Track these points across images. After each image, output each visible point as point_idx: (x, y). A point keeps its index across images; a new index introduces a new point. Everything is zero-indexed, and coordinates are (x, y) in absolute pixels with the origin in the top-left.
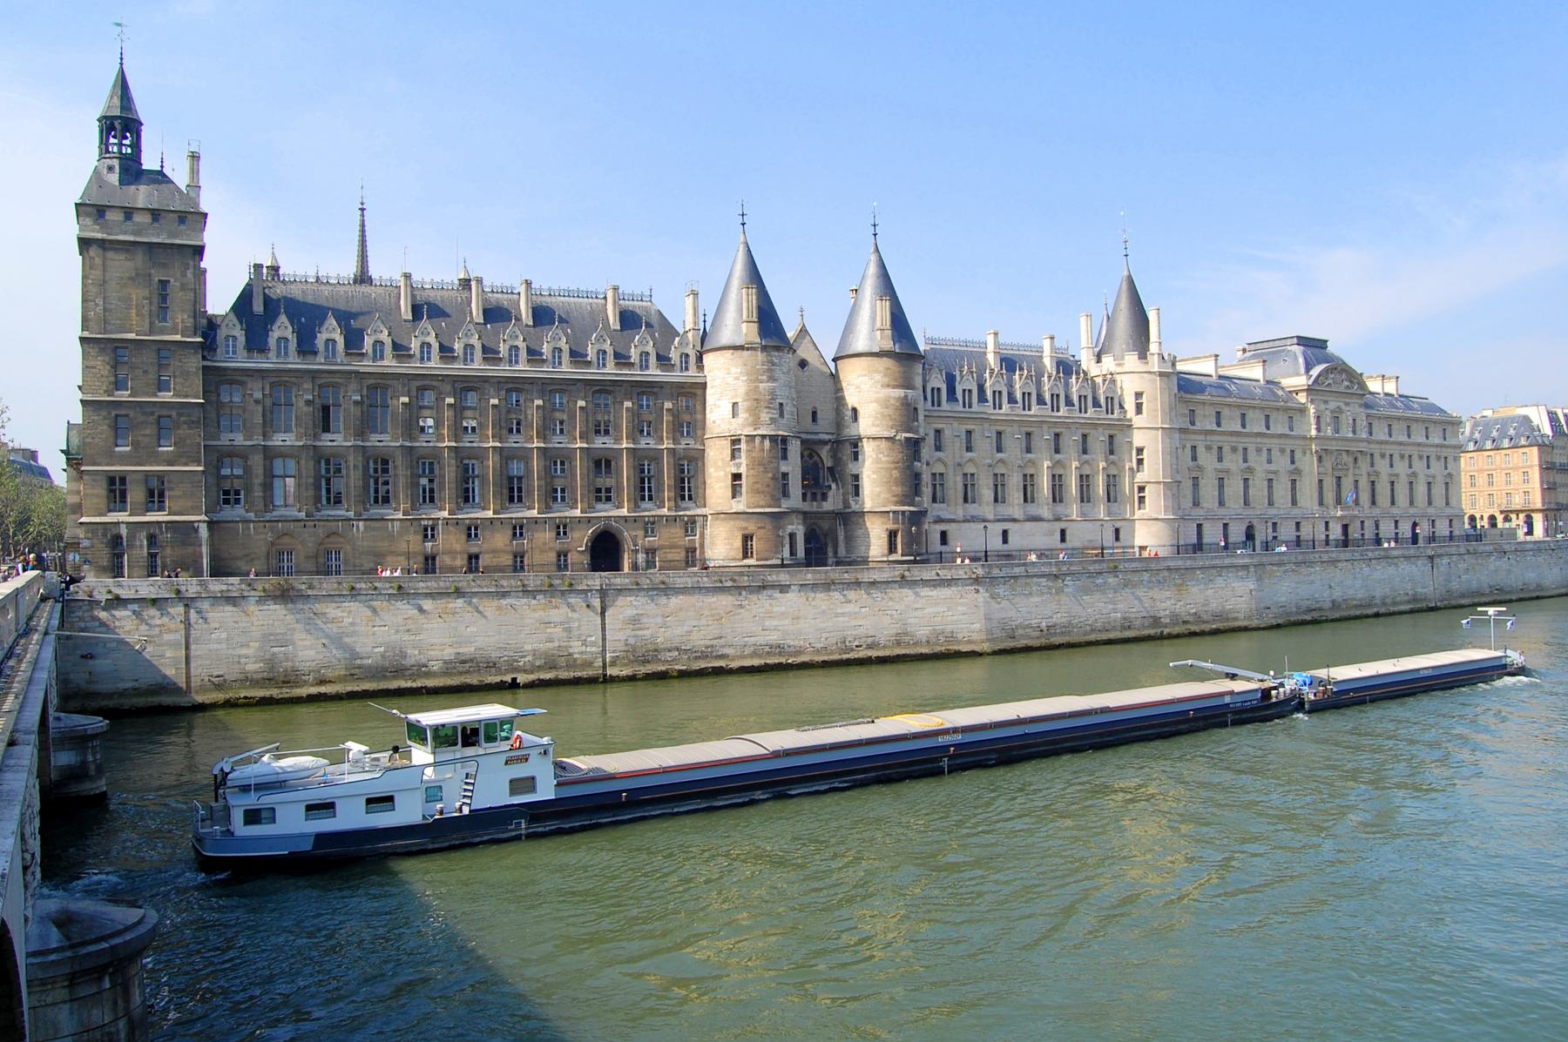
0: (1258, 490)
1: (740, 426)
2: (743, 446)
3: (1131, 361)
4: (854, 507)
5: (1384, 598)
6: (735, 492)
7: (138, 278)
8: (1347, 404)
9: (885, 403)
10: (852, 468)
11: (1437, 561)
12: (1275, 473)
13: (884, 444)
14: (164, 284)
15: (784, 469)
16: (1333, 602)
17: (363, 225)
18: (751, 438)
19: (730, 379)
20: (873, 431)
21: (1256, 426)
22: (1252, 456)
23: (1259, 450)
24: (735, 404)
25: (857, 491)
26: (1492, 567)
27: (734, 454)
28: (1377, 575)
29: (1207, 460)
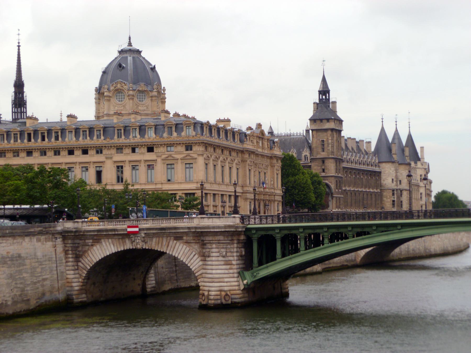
1: (393, 186)
2: (395, 192)
7: (337, 140)
18: (397, 190)
24: (393, 179)
27: (393, 194)
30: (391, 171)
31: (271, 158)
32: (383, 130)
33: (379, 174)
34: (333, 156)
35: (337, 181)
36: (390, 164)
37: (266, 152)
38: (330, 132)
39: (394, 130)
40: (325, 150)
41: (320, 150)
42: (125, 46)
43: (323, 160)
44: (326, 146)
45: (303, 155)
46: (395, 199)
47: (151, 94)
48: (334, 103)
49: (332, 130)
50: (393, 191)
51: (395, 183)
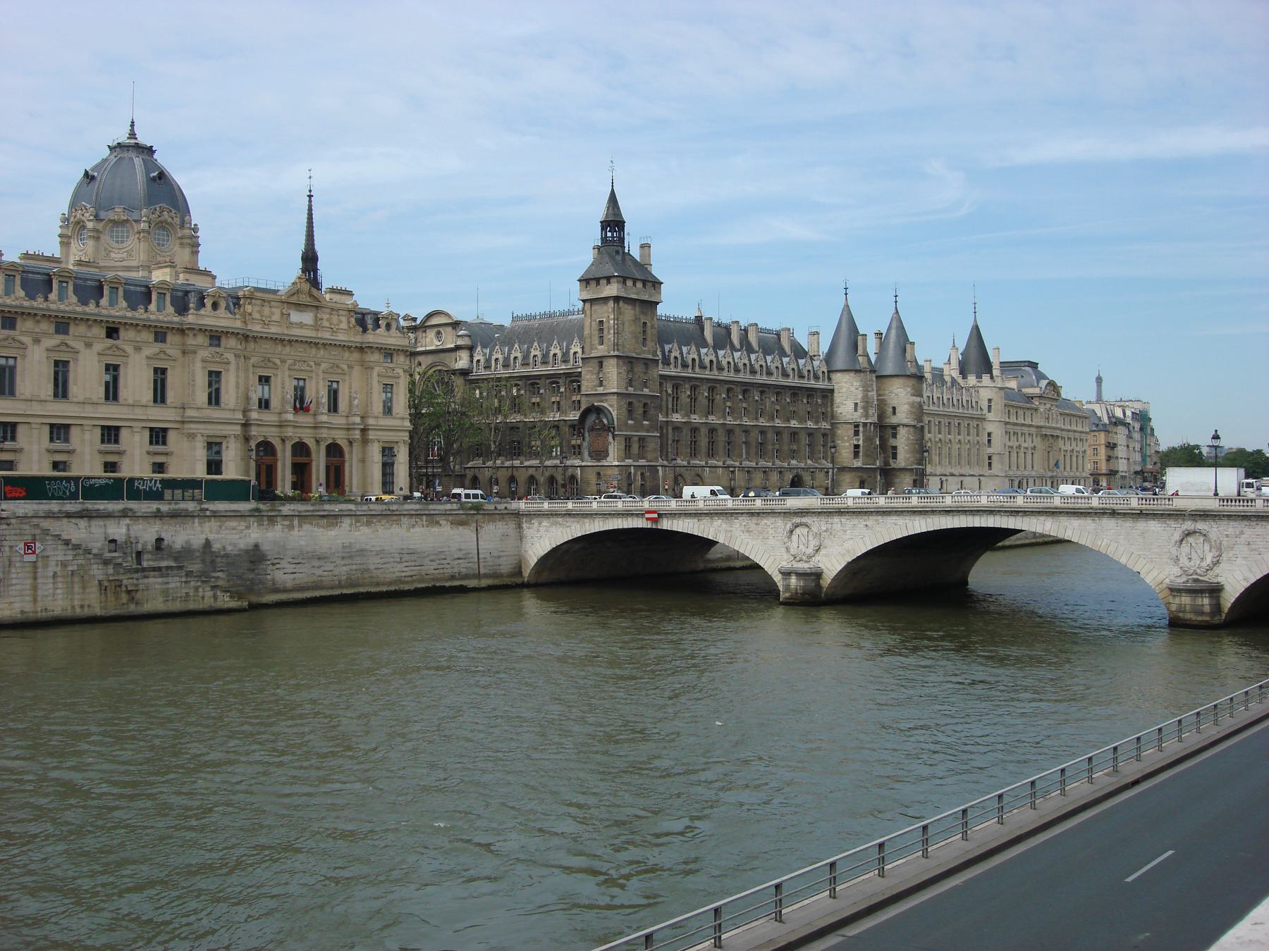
1: (858, 417)
2: (861, 429)
3: (986, 378)
4: (893, 466)
6: (856, 454)
7: (636, 320)
9: (912, 405)
10: (892, 442)
13: (912, 430)
14: (645, 324)
17: (310, 209)
18: (865, 424)
19: (852, 389)
20: (905, 421)
25: (895, 456)
27: (856, 433)
30: (852, 389)
31: (361, 349)
32: (847, 310)
33: (828, 394)
34: (616, 353)
35: (630, 404)
36: (852, 374)
37: (341, 337)
38: (611, 304)
39: (893, 310)
40: (605, 341)
41: (596, 340)
42: (123, 137)
43: (600, 361)
44: (605, 331)
45: (572, 352)
46: (861, 443)
47: (136, 227)
48: (645, 247)
49: (617, 299)
50: (857, 426)
51: (860, 411)
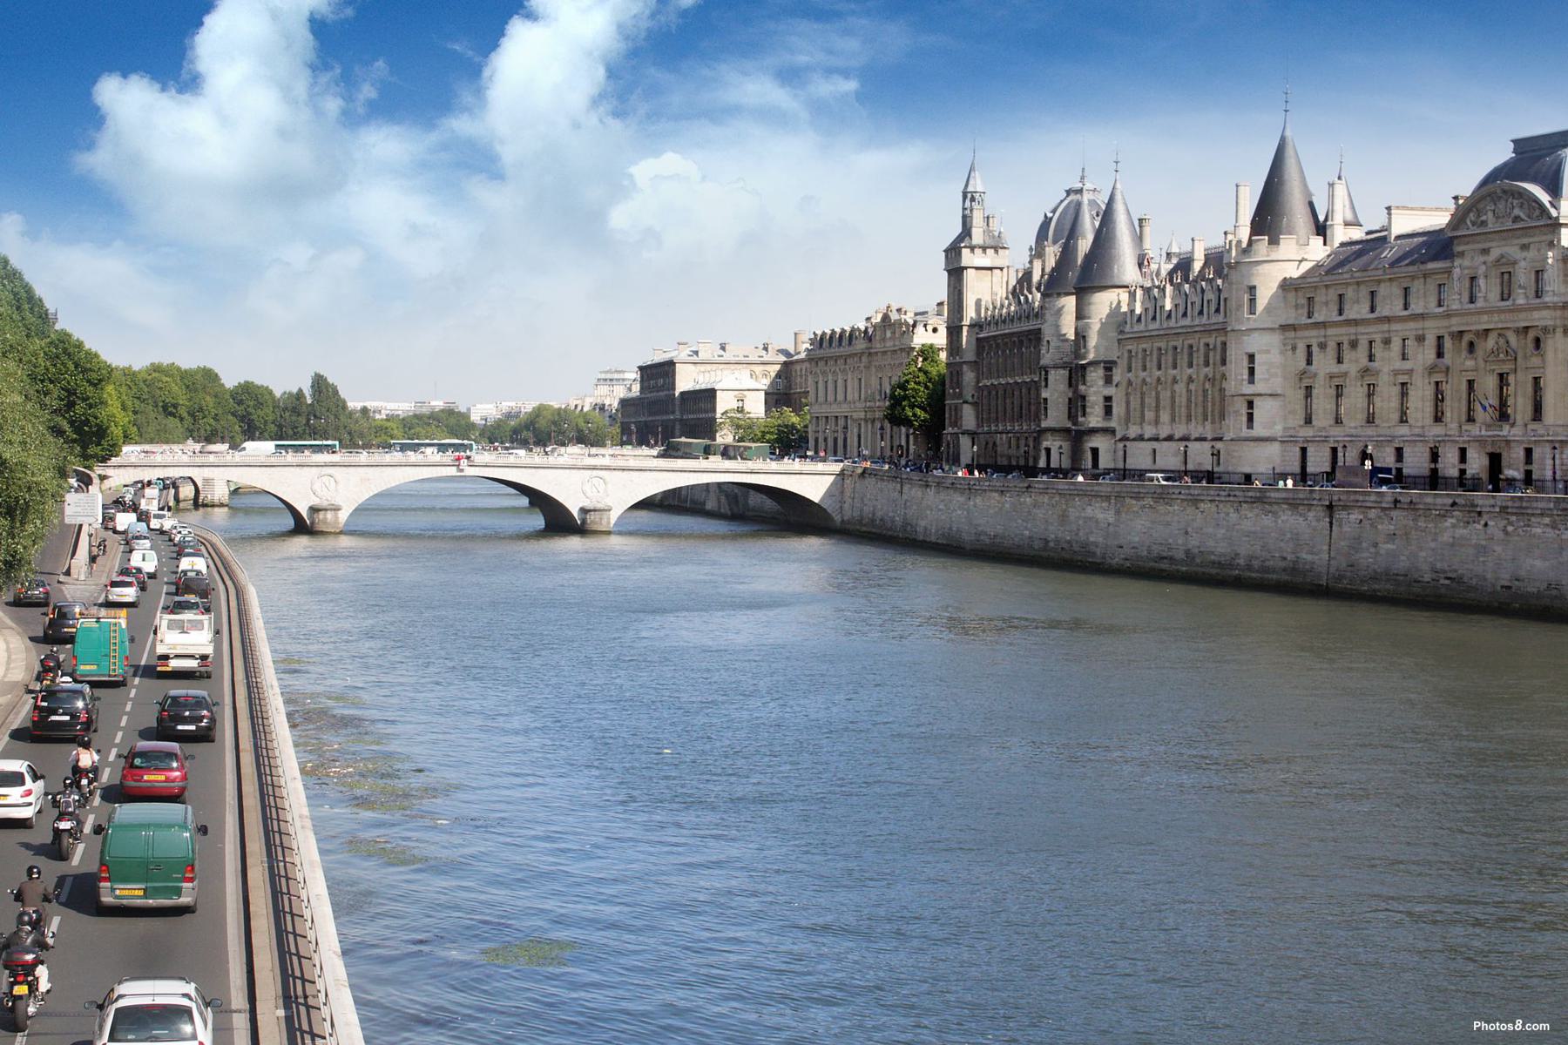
0: (1387, 402)
5: (1251, 558)
8: (1525, 247)
11: (1340, 515)
12: (1410, 372)
15: (1044, 395)
16: (1187, 552)
21: (1391, 304)
22: (1378, 350)
23: (1387, 342)
26: (1446, 537)
28: (1247, 525)
29: (1324, 364)
